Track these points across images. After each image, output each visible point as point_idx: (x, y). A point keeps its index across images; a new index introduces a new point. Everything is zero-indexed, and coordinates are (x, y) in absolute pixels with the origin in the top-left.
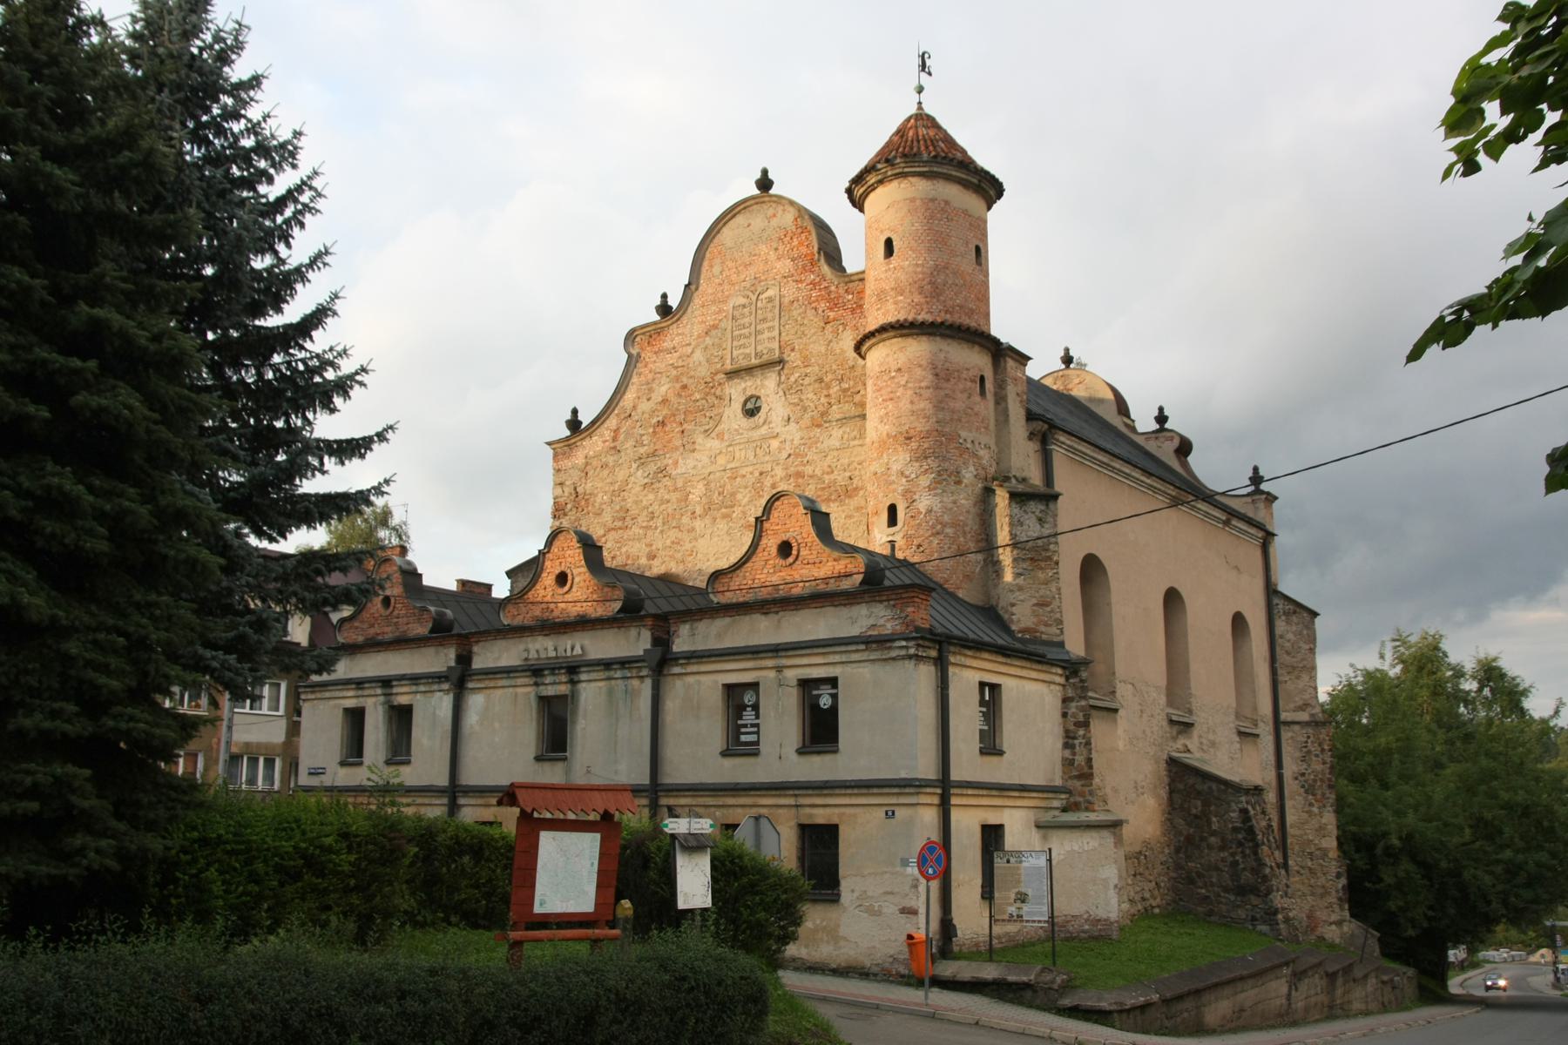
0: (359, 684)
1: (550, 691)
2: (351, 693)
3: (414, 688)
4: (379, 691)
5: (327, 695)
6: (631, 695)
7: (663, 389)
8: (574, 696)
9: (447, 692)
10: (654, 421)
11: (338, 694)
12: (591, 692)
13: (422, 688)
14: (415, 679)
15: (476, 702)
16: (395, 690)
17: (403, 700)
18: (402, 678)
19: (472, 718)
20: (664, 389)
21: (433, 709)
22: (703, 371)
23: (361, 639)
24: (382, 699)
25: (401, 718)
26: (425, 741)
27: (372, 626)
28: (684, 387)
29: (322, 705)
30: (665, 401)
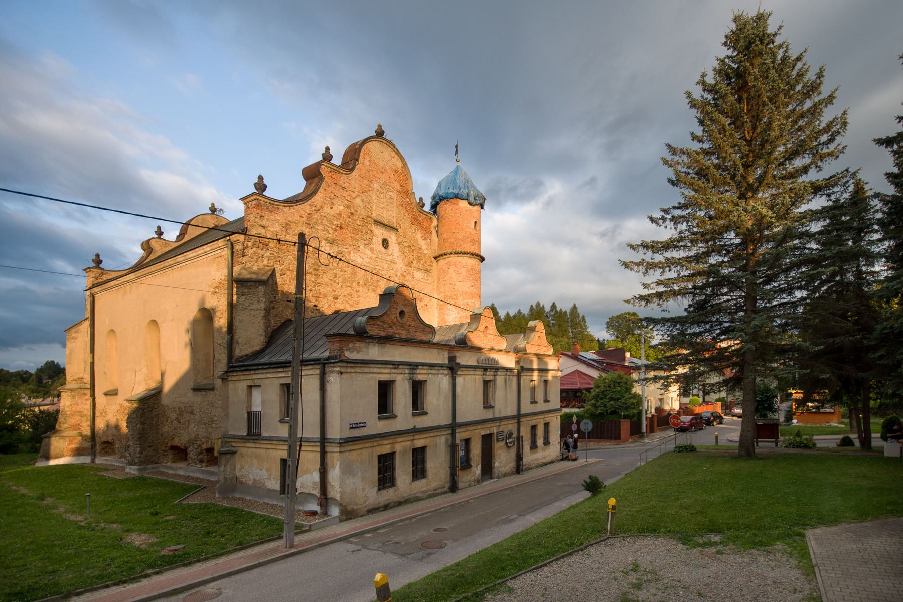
0: (396, 365)
1: (488, 378)
2: (387, 371)
3: (430, 371)
4: (407, 371)
5: (366, 370)
6: (511, 381)
7: (339, 207)
8: (494, 381)
9: (446, 375)
10: (335, 222)
11: (376, 370)
12: (500, 379)
13: (434, 372)
14: (432, 366)
15: (459, 380)
16: (418, 371)
17: (420, 377)
18: (423, 364)
19: (458, 390)
20: (341, 208)
21: (438, 386)
22: (362, 213)
23: (383, 334)
24: (407, 376)
25: (417, 388)
26: (435, 401)
27: (391, 327)
28: (352, 214)
29: (359, 377)
30: (340, 215)
